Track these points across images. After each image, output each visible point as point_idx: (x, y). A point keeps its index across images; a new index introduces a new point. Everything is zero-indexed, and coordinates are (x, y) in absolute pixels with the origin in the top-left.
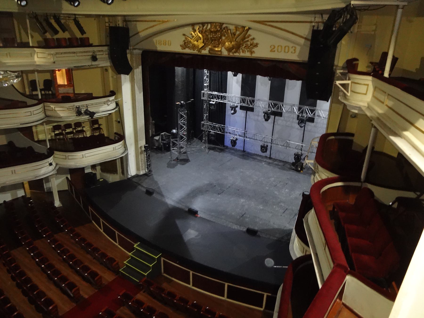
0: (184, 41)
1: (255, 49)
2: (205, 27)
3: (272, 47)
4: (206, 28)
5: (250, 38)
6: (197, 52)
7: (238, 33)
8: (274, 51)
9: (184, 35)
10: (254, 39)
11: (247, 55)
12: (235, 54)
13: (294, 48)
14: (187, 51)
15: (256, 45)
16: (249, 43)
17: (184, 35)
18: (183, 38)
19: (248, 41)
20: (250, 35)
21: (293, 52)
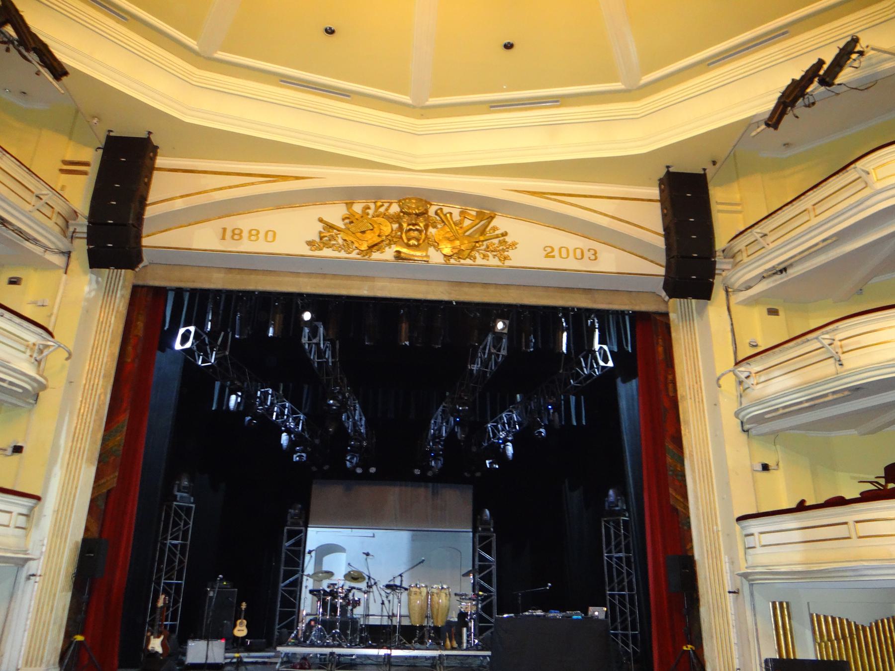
0: (320, 232)
1: (510, 253)
2: (382, 210)
3: (549, 250)
4: (387, 210)
5: (497, 232)
6: (359, 256)
7: (467, 223)
8: (553, 257)
9: (321, 220)
10: (505, 234)
11: (493, 261)
12: (462, 261)
13: (592, 252)
14: (327, 252)
15: (514, 245)
16: (496, 241)
17: (321, 220)
18: (320, 227)
19: (497, 237)
20: (495, 229)
21: (593, 257)
